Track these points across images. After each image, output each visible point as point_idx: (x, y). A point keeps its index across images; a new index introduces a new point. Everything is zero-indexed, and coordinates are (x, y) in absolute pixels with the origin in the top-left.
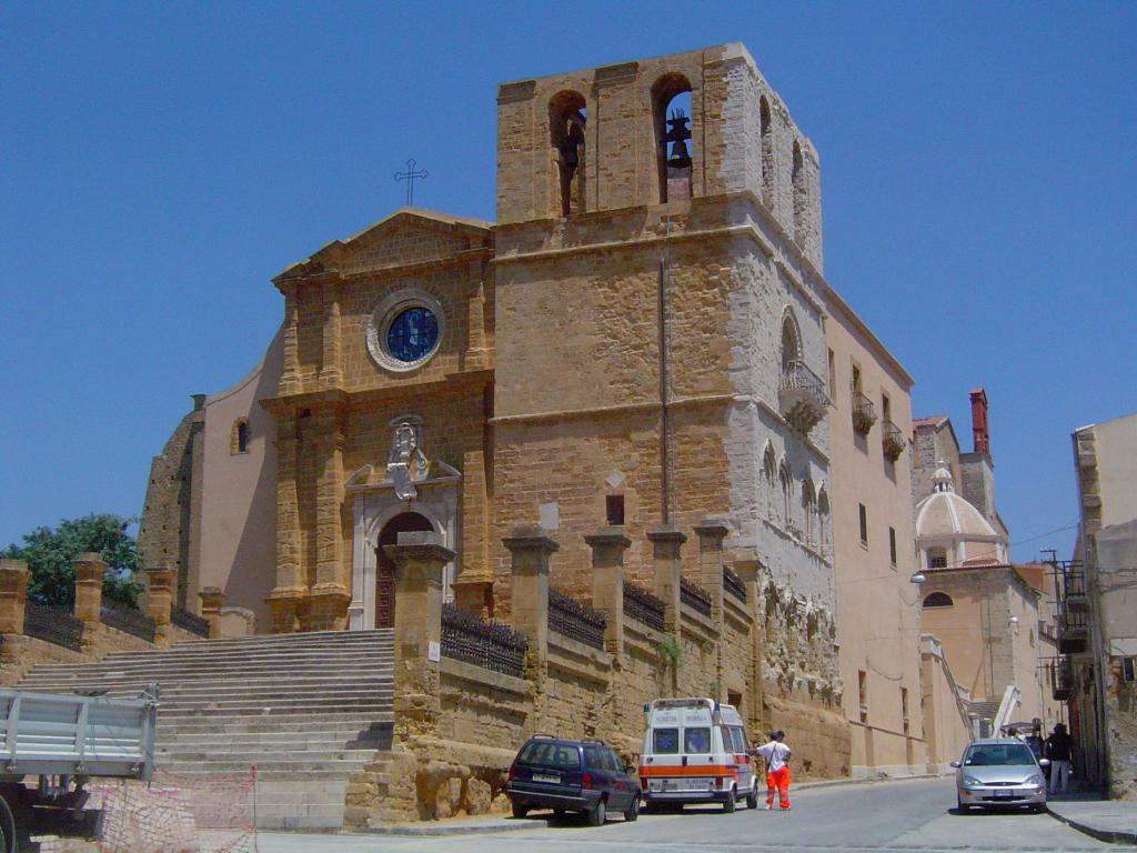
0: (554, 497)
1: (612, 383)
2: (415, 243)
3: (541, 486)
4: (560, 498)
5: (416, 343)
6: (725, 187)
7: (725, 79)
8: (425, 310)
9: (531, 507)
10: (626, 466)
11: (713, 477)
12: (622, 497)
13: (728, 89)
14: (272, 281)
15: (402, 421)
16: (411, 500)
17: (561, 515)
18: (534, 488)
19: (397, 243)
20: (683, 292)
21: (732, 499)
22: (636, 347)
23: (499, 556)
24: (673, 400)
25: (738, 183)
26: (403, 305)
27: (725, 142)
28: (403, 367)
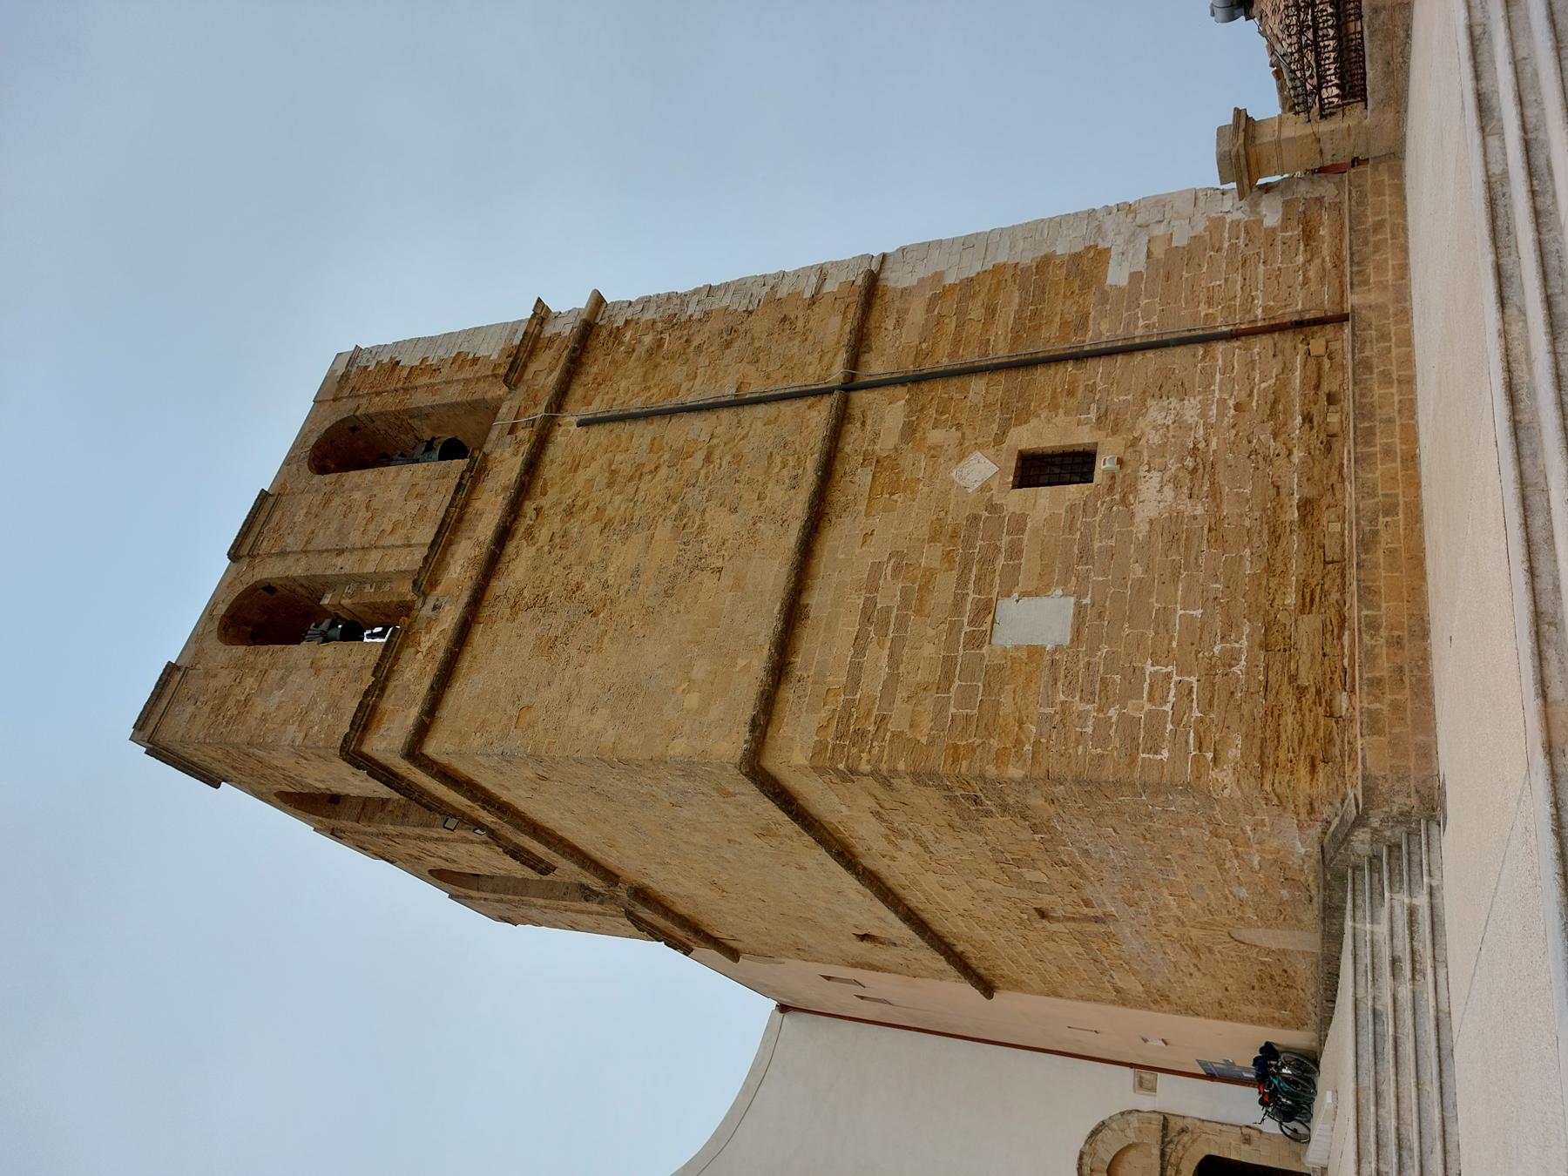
0: (986, 609)
3: (951, 644)
9: (1001, 668)
11: (1022, 288)
18: (949, 662)
21: (1080, 248)
22: (708, 459)
23: (1133, 761)
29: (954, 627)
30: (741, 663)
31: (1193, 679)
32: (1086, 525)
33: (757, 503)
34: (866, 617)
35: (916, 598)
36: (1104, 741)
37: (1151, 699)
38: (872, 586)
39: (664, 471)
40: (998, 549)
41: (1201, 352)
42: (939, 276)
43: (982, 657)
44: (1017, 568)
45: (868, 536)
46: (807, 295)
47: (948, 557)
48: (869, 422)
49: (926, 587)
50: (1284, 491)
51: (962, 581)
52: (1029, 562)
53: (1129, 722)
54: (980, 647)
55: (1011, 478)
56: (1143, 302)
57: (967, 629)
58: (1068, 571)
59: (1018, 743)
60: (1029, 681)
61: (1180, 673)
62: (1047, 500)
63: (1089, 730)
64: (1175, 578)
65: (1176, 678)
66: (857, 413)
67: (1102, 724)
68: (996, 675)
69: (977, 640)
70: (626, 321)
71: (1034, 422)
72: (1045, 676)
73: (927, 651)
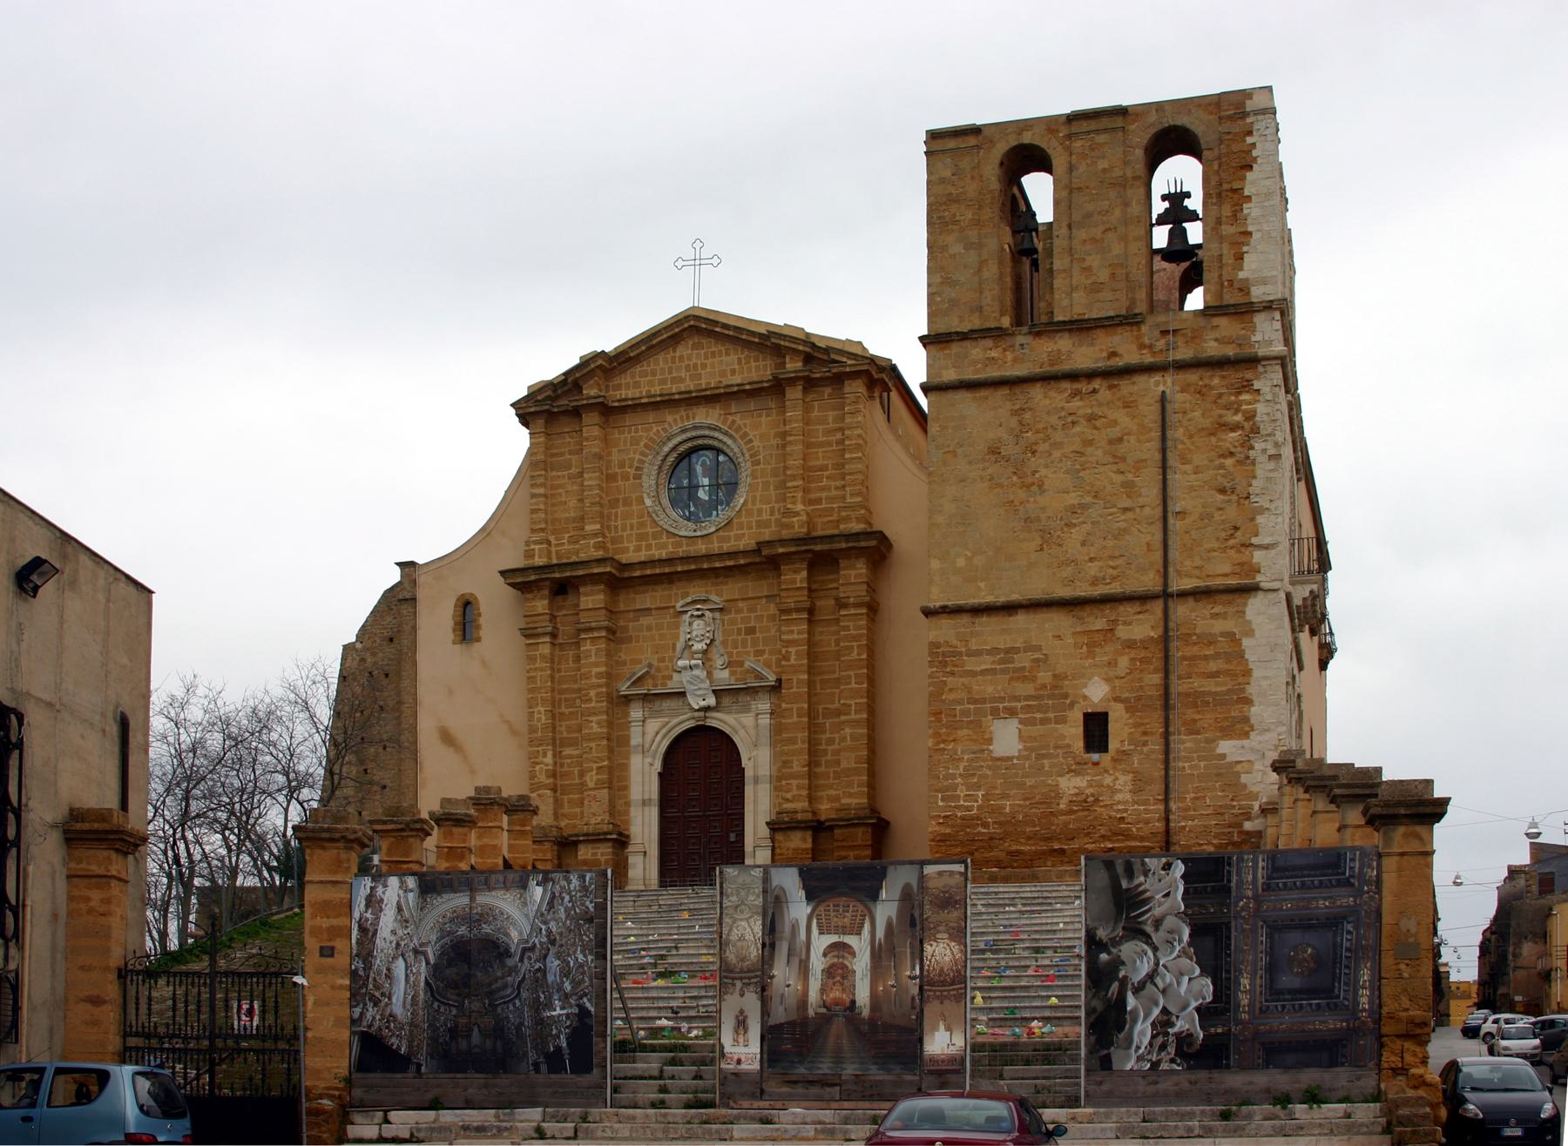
0: (1012, 713)
1: (1091, 560)
2: (706, 358)
3: (993, 700)
4: (1020, 716)
5: (707, 498)
6: (1248, 293)
7: (1249, 140)
8: (719, 451)
9: (981, 727)
10: (1112, 674)
12: (1106, 714)
13: (1255, 153)
14: (512, 405)
15: (694, 602)
16: (707, 709)
17: (1021, 737)
18: (984, 701)
19: (681, 358)
20: (1191, 437)
22: (1126, 510)
24: (1176, 585)
25: (1268, 289)
26: (690, 444)
27: (1250, 229)
28: (687, 529)
29: (1002, 699)
30: (982, 585)
31: (975, 811)
32: (1058, 755)
33: (1087, 558)
34: (1008, 651)
35: (1022, 676)
36: (946, 777)
37: (966, 795)
38: (1029, 648)
39: (1118, 478)
40: (1046, 712)
41: (1160, 797)
42: (1250, 633)
43: (986, 716)
44: (1034, 724)
45: (1059, 637)
46: (1254, 541)
47: (1044, 686)
48: (1140, 616)
49: (1024, 679)
50: (1070, 842)
51: (1028, 698)
52: (1037, 730)
53: (955, 787)
54: (991, 715)
55: (1090, 711)
56: (1202, 764)
57: (1001, 706)
58: (1031, 749)
59: (944, 741)
60: (975, 741)
61: (979, 808)
62: (1073, 732)
63: (951, 771)
64: (1025, 800)
65: (976, 804)
66: (1148, 606)
67: (953, 777)
68: (977, 725)
69: (995, 713)
70: (1259, 390)
71: (1128, 715)
72: (975, 748)
73: (987, 688)
